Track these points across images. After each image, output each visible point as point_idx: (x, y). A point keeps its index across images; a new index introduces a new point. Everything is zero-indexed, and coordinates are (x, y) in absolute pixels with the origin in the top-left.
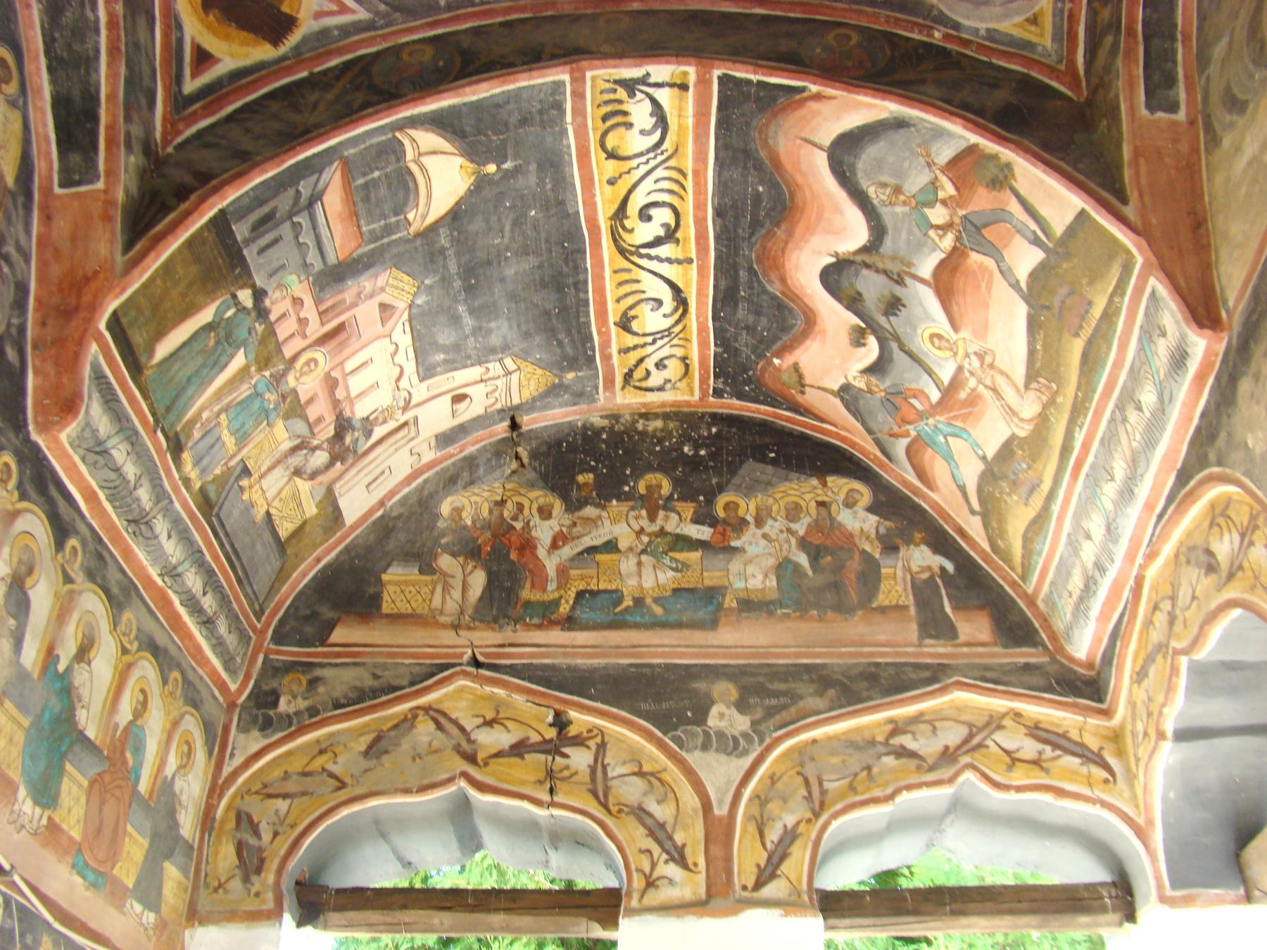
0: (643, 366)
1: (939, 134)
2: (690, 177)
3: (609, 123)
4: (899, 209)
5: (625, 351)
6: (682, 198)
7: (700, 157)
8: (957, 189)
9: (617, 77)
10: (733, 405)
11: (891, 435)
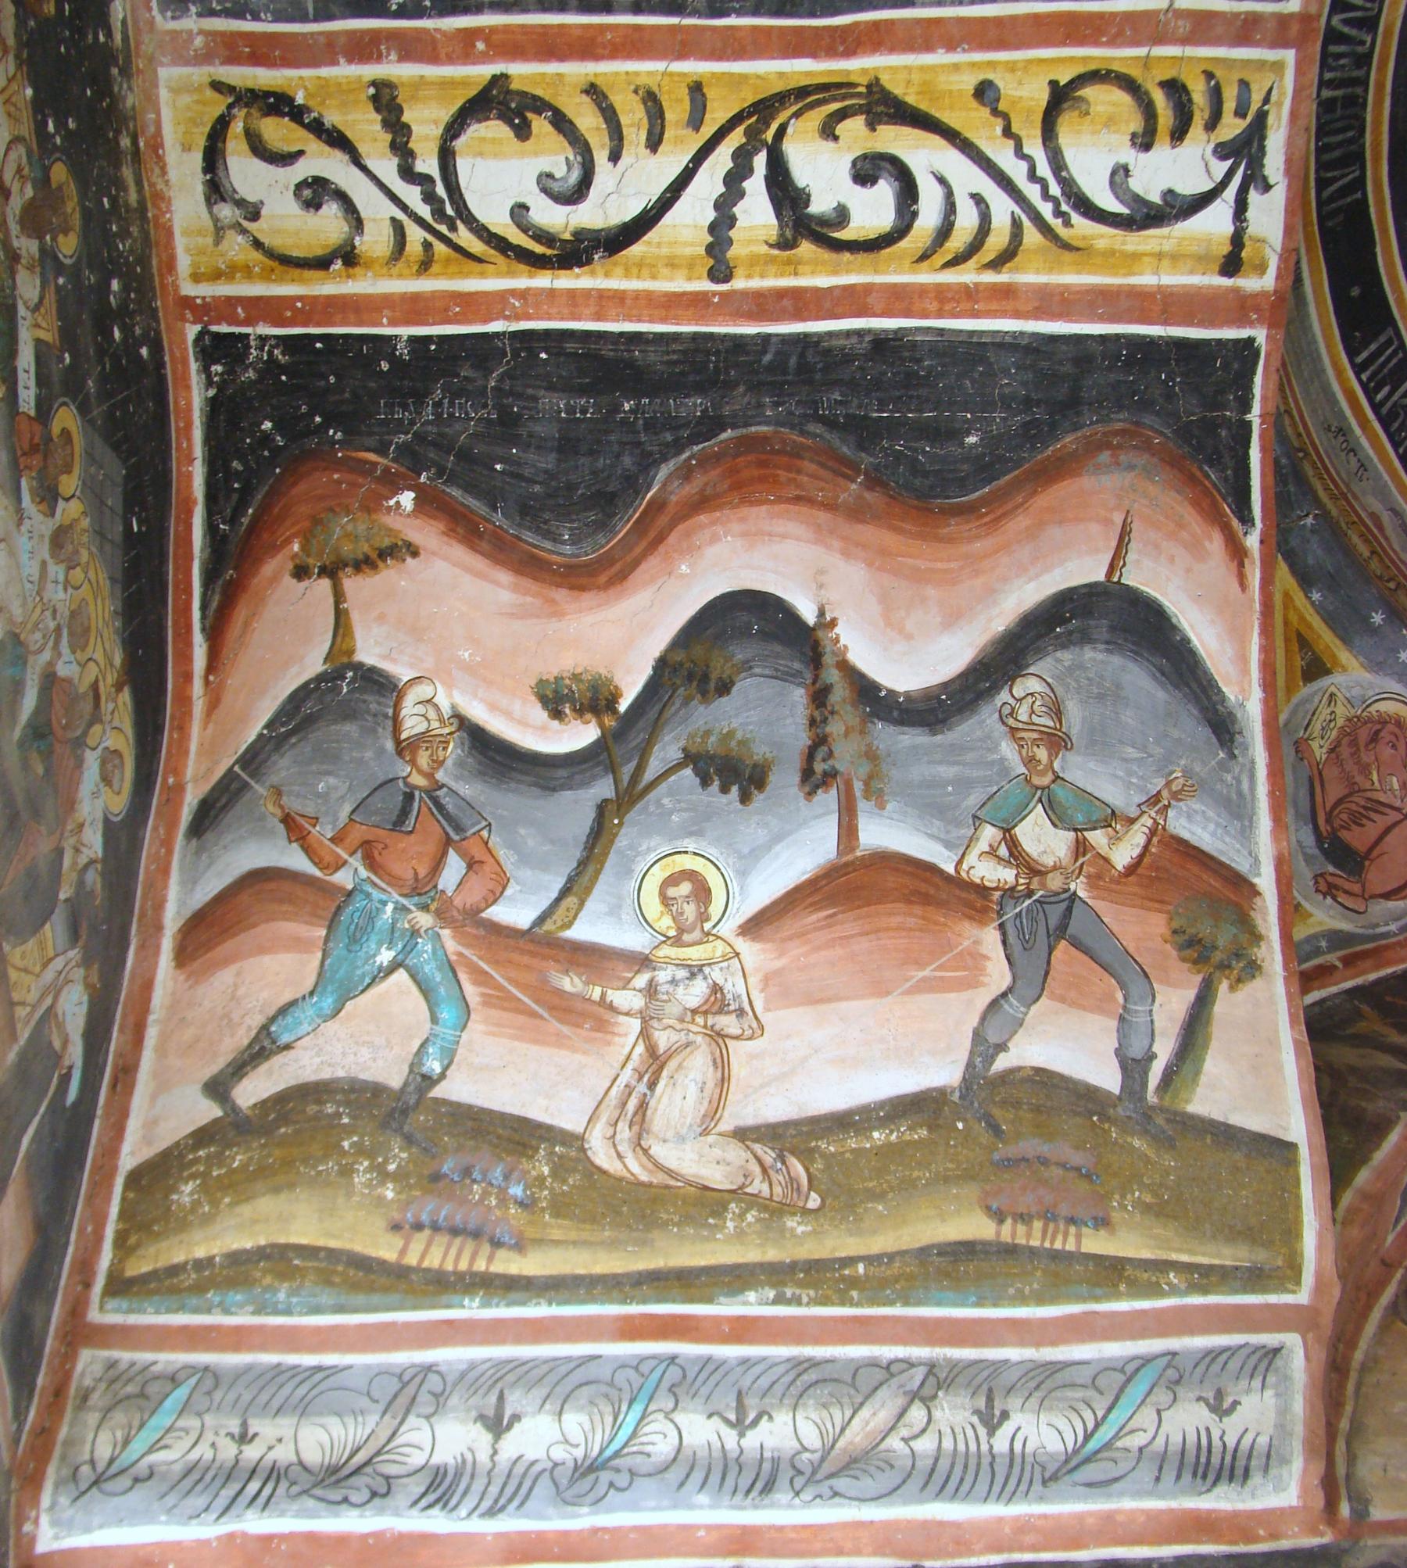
0: (313, 145)
1: (1238, 810)
2: (990, 277)
3: (1159, 98)
4: (1008, 750)
5: (386, 101)
6: (924, 257)
7: (1050, 302)
8: (1132, 869)
9: (1271, 120)
10: (193, 395)
11: (288, 820)
